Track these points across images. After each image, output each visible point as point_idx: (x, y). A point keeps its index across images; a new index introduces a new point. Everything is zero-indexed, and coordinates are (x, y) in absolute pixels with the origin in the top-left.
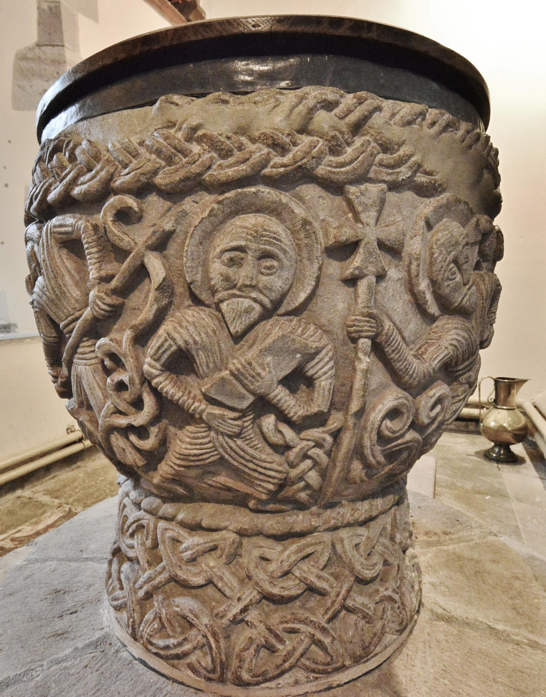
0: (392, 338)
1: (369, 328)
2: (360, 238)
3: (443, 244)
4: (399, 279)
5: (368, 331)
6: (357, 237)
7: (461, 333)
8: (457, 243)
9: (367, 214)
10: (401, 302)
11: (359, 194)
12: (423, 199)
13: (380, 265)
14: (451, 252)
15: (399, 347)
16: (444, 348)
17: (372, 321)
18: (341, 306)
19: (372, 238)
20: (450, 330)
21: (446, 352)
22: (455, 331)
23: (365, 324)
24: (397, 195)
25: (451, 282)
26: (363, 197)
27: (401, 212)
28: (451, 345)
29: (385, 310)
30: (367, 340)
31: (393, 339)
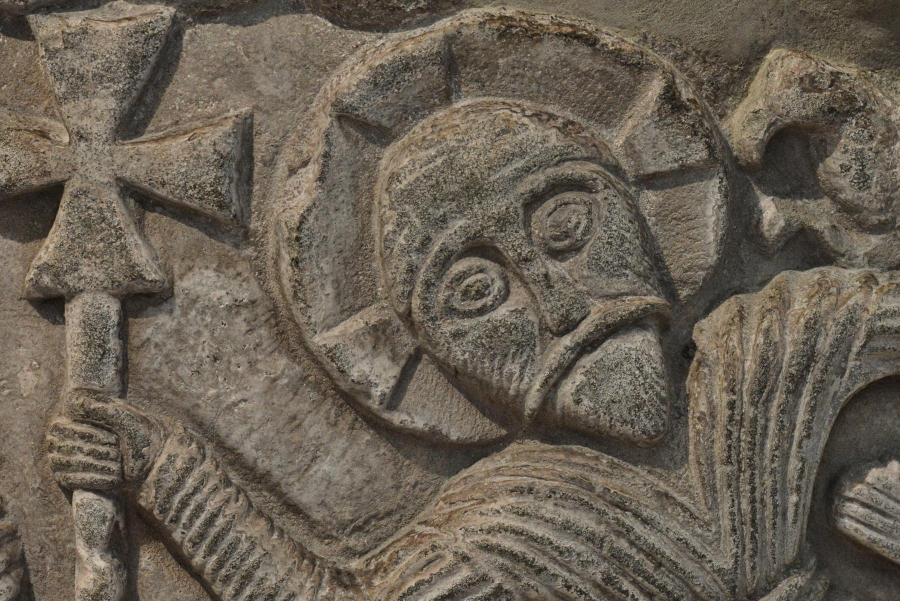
0: (177, 499)
1: (90, 460)
2: (56, 177)
3: (409, 194)
4: (237, 307)
5: (87, 468)
6: (46, 173)
7: (548, 509)
8: (474, 189)
9: (82, 105)
10: (258, 383)
11: (59, 45)
12: (354, 36)
13: (119, 262)
14: (444, 220)
15: (213, 532)
16: (450, 558)
17: (101, 435)
18: (29, 380)
19: (96, 176)
20: (493, 496)
21: (464, 573)
22: (512, 500)
23: (79, 443)
24: (236, 31)
25: (467, 323)
26: (70, 54)
27: (250, 86)
28: (487, 548)
29: (187, 404)
30: (90, 496)
31: (184, 504)
